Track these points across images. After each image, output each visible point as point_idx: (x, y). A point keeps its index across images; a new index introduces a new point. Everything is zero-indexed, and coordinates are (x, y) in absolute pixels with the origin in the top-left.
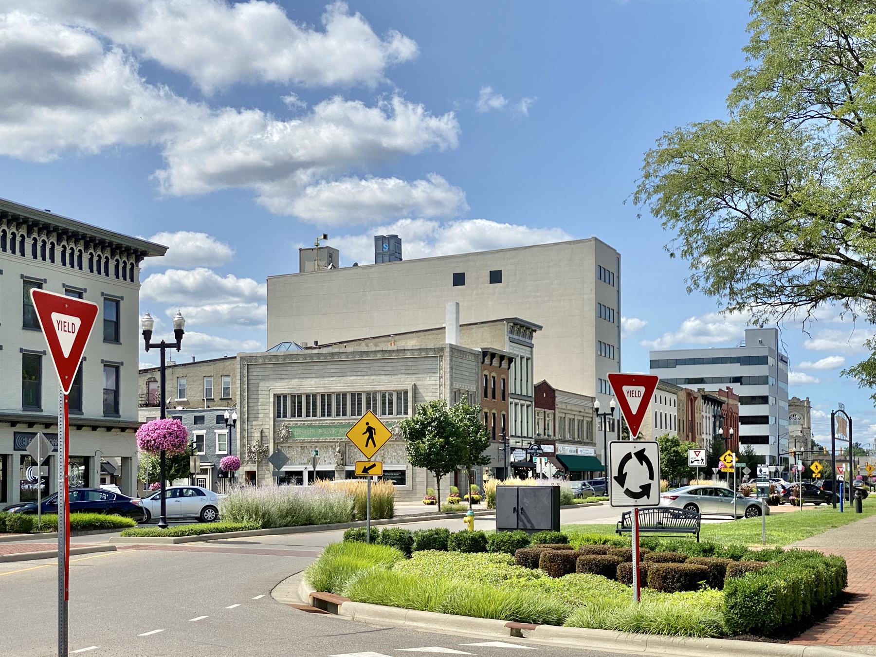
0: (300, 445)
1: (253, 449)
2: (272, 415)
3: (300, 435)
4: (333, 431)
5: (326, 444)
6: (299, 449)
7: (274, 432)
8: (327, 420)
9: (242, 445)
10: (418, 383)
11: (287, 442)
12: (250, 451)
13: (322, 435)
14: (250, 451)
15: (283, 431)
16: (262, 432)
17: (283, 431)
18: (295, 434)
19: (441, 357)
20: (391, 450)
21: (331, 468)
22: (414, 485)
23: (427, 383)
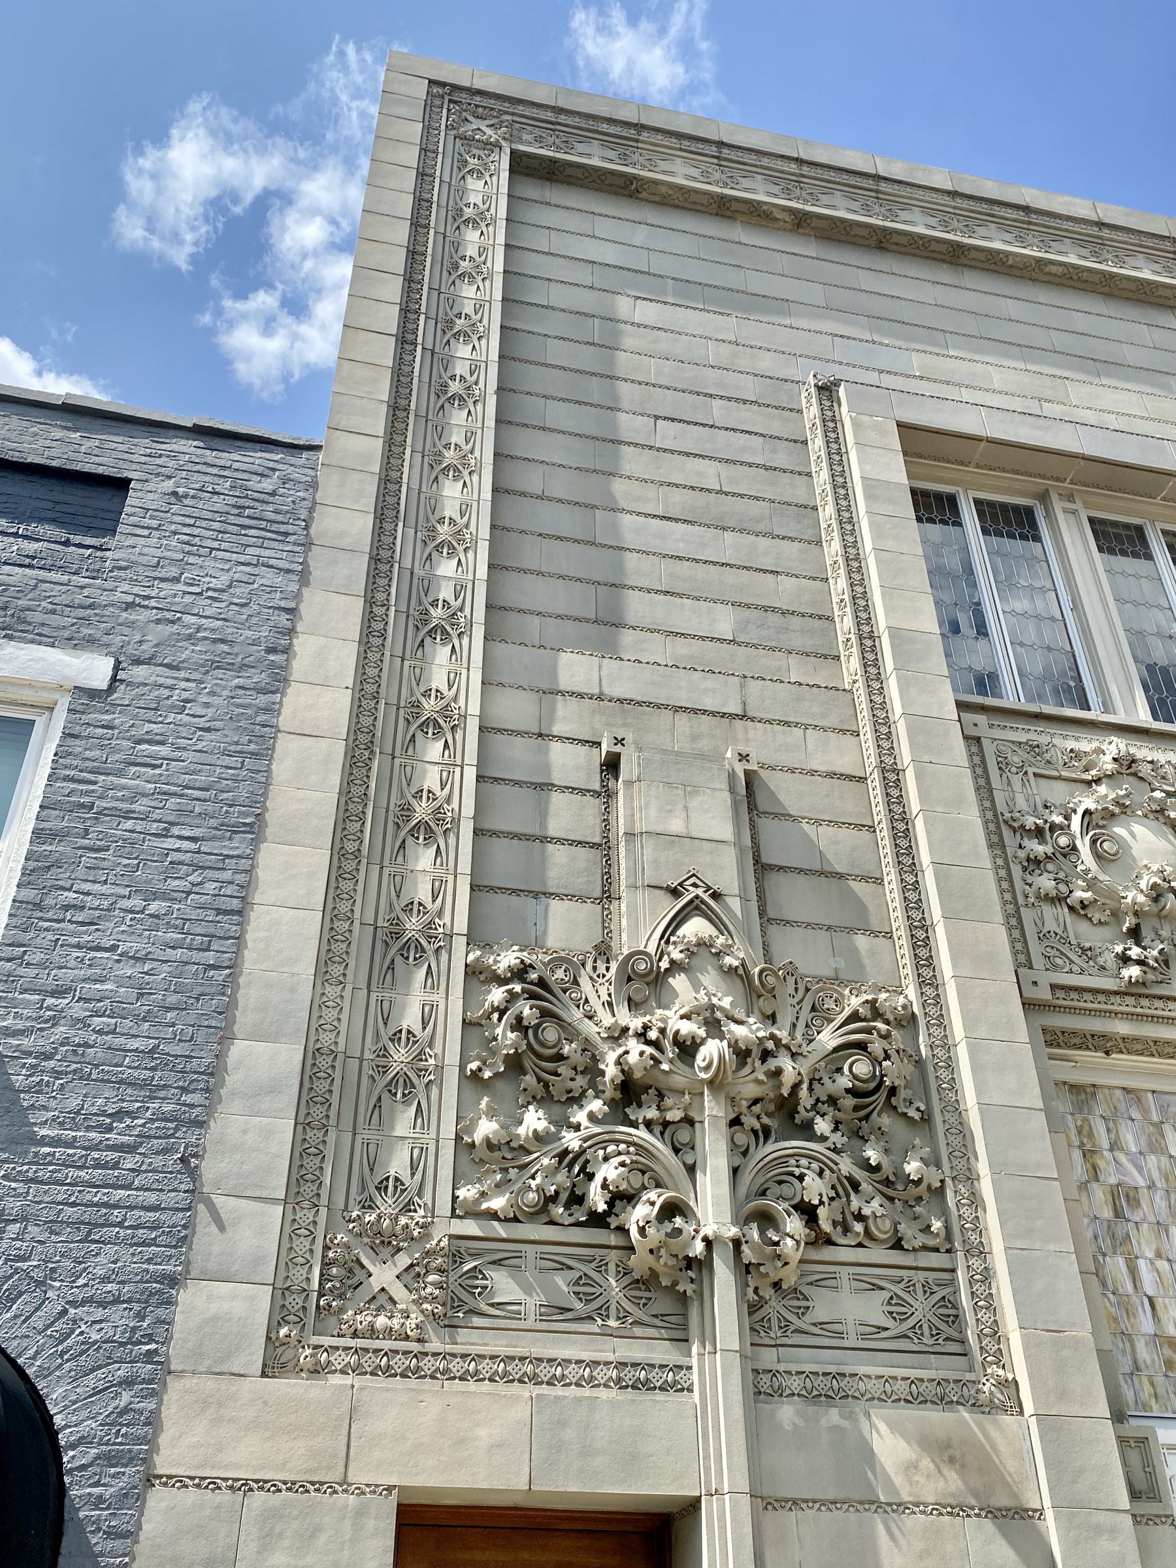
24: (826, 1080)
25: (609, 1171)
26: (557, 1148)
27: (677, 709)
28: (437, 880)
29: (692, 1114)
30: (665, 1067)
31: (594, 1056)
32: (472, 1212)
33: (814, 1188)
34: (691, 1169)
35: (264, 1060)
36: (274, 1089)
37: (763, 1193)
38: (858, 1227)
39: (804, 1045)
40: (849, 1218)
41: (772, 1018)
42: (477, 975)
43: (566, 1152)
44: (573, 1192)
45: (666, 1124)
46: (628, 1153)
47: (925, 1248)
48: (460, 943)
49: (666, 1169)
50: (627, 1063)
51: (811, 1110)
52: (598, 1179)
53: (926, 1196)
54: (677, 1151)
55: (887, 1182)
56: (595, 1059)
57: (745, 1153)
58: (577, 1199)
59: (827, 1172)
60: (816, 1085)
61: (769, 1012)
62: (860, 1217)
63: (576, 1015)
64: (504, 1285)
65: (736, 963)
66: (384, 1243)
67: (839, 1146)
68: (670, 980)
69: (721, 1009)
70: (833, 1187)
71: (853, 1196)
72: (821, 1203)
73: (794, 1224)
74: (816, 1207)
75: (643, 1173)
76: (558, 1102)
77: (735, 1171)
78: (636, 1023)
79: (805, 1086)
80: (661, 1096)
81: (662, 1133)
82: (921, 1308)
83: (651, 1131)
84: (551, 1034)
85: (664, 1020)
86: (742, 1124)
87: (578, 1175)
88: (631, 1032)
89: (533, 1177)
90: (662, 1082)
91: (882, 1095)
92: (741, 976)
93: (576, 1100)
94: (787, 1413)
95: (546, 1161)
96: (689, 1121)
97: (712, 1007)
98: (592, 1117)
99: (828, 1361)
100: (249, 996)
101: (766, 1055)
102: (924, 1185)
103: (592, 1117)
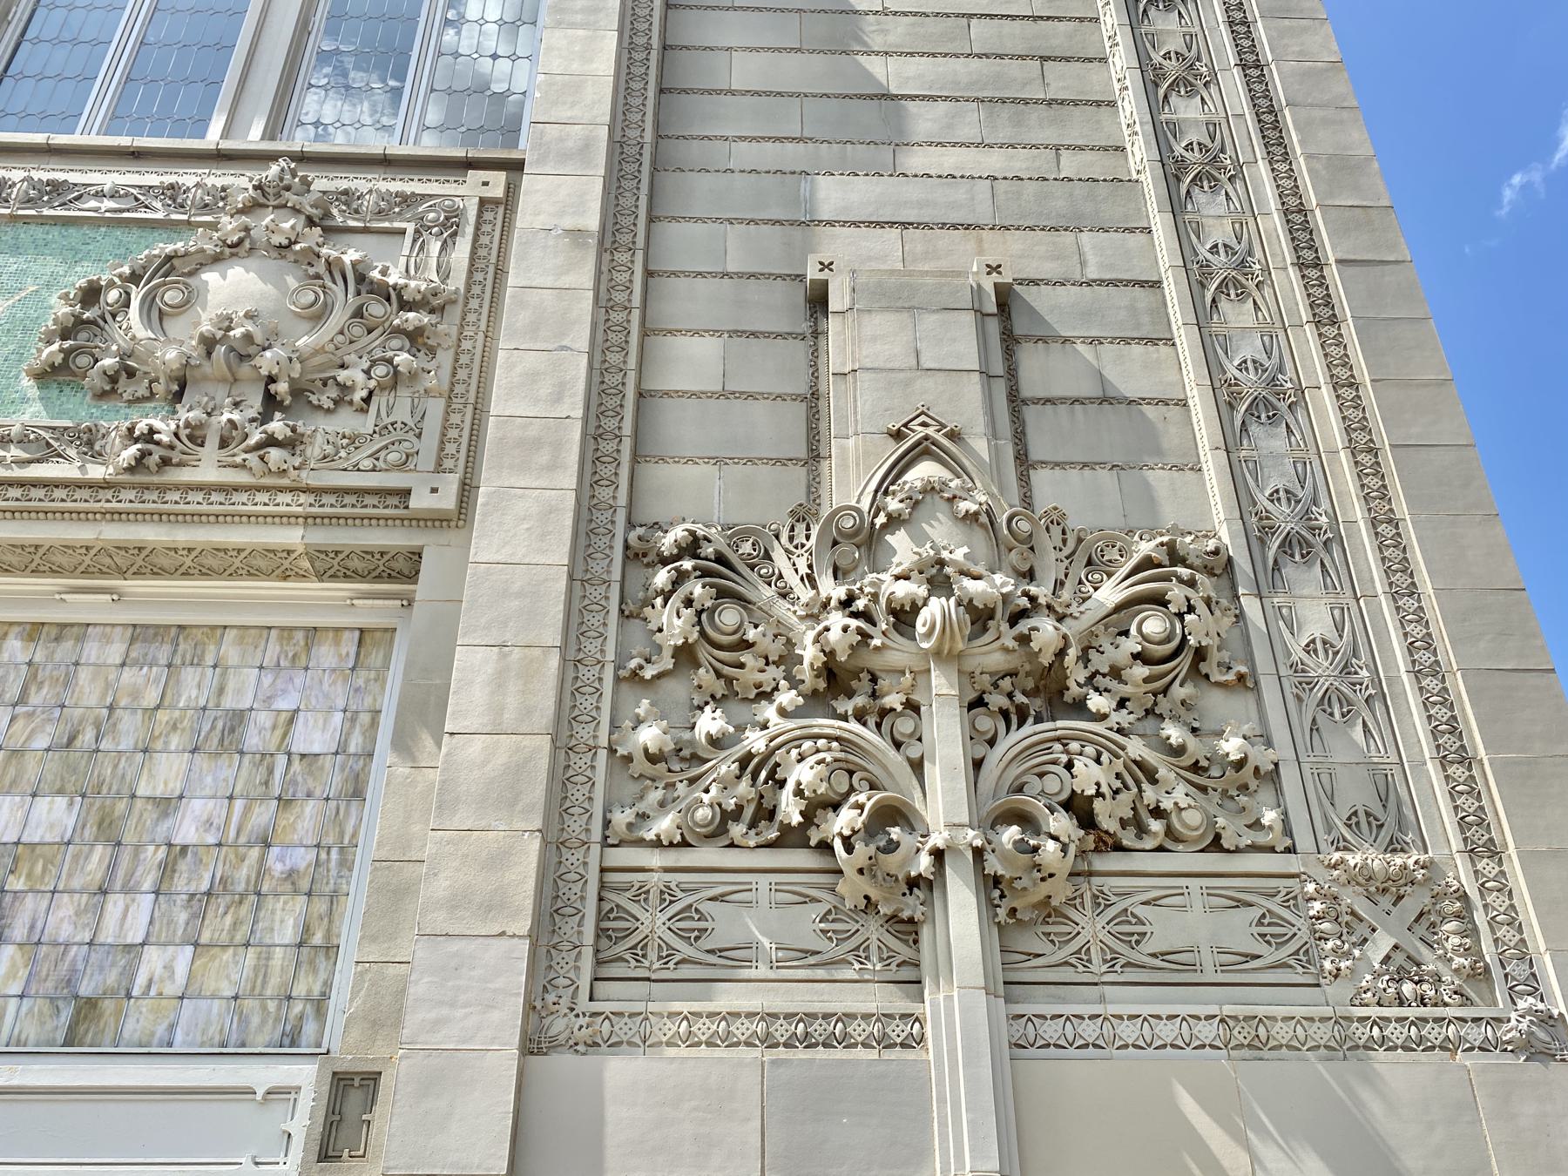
24: (1107, 647)
25: (804, 774)
26: (738, 751)
29: (915, 697)
30: (876, 642)
31: (789, 641)
34: (917, 766)
37: (1020, 790)
38: (1156, 826)
39: (1075, 604)
40: (1144, 814)
41: (1030, 575)
43: (749, 756)
44: (760, 804)
45: (884, 712)
46: (829, 749)
47: (1254, 848)
49: (885, 768)
50: (828, 642)
51: (1085, 684)
52: (790, 786)
53: (1253, 784)
54: (898, 745)
55: (1196, 768)
56: (790, 643)
57: (992, 742)
58: (767, 813)
59: (1105, 757)
60: (1093, 654)
61: (1026, 568)
62: (1157, 813)
65: (974, 508)
67: (1126, 726)
68: (888, 537)
69: (954, 563)
70: (1118, 776)
71: (1145, 786)
72: (1099, 794)
73: (1061, 823)
74: (1090, 799)
75: (851, 773)
77: (978, 764)
78: (840, 593)
79: (1073, 653)
80: (874, 679)
81: (878, 725)
83: (864, 724)
84: (730, 616)
85: (877, 584)
86: (986, 705)
87: (766, 782)
88: (833, 603)
89: (707, 791)
90: (876, 662)
91: (1185, 661)
92: (982, 526)
93: (766, 696)
95: (723, 769)
96: (912, 707)
97: (941, 563)
98: (783, 712)
101: (1015, 618)
102: (1248, 770)
103: (783, 712)
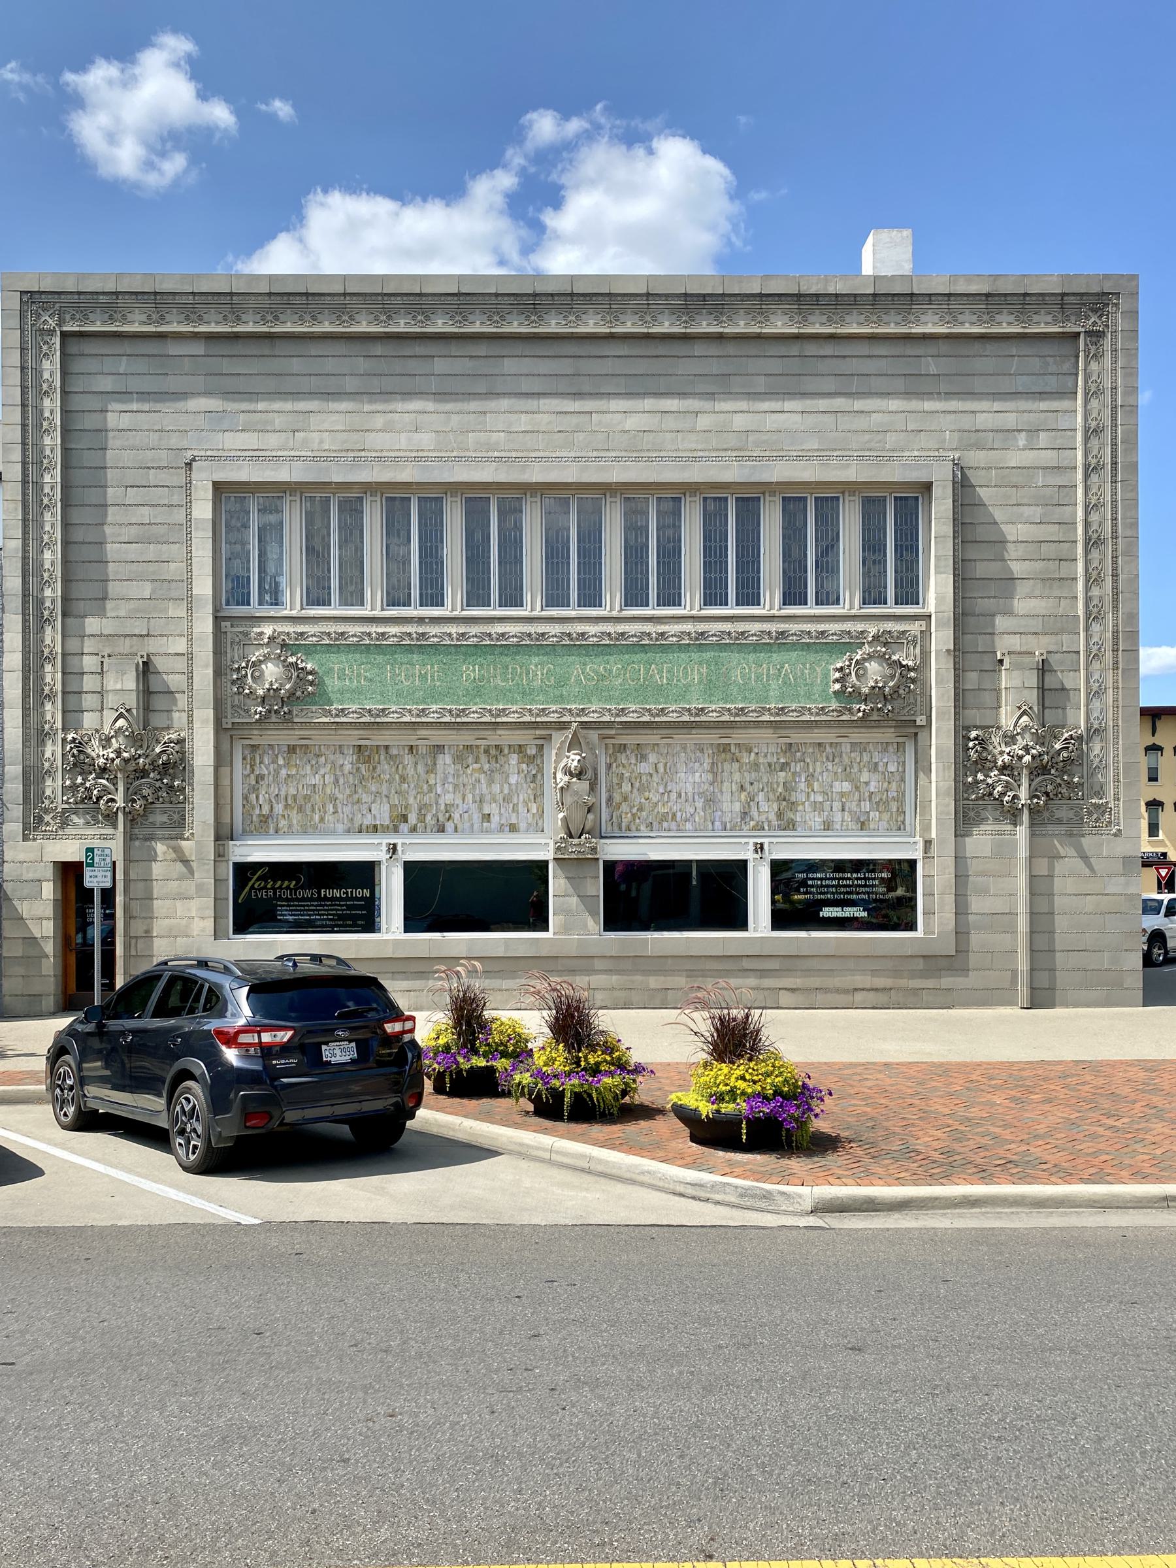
0: (352, 738)
1: (98, 753)
2: (203, 587)
3: (352, 688)
4: (537, 669)
5: (493, 738)
6: (347, 762)
7: (219, 673)
8: (502, 621)
9: (35, 735)
10: (975, 458)
11: (287, 722)
12: (79, 763)
13: (476, 692)
14: (79, 763)
15: (272, 672)
16: (146, 670)
17: (272, 672)
18: (333, 684)
19: (1096, 336)
20: (824, 771)
21: (536, 846)
22: (961, 932)
23: (1015, 458)
27: (126, 636)
28: (52, 712)
32: (67, 803)
33: (145, 792)
35: (14, 770)
36: (16, 778)
42: (64, 740)
48: (60, 731)
63: (89, 751)
64: (75, 818)
66: (46, 811)
76: (85, 774)
82: (176, 817)
84: (82, 757)
94: (137, 843)
99: (149, 831)
100: (7, 755)
